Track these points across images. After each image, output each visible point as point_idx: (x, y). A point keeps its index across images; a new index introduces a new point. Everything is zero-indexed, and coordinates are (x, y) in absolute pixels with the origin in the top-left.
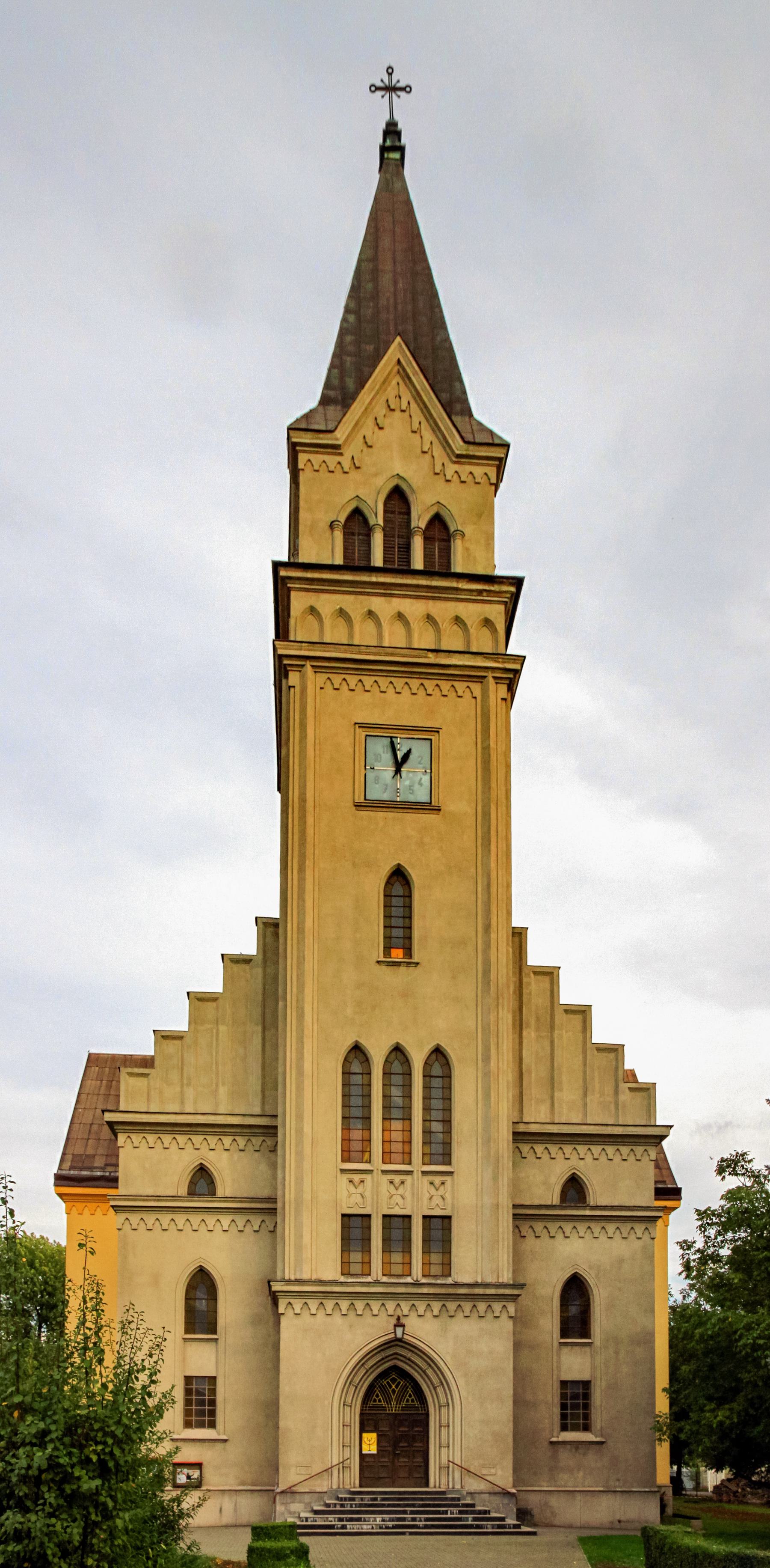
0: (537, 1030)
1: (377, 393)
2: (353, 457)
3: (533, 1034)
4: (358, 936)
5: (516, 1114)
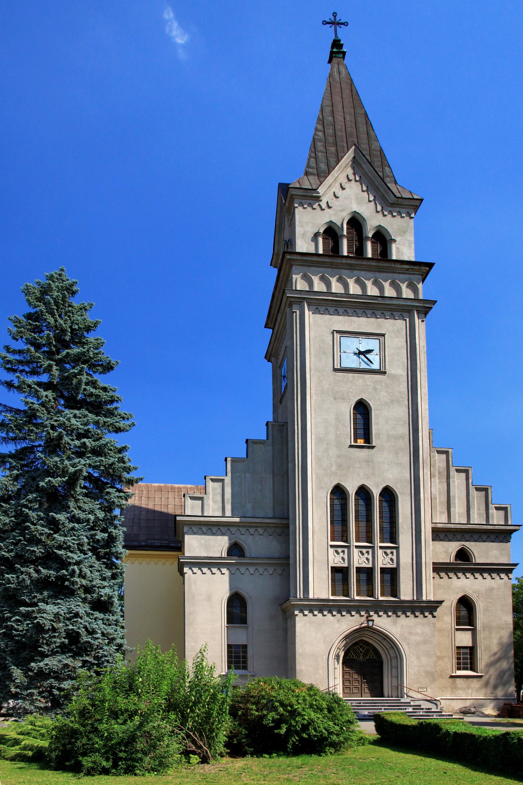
2: (327, 202)
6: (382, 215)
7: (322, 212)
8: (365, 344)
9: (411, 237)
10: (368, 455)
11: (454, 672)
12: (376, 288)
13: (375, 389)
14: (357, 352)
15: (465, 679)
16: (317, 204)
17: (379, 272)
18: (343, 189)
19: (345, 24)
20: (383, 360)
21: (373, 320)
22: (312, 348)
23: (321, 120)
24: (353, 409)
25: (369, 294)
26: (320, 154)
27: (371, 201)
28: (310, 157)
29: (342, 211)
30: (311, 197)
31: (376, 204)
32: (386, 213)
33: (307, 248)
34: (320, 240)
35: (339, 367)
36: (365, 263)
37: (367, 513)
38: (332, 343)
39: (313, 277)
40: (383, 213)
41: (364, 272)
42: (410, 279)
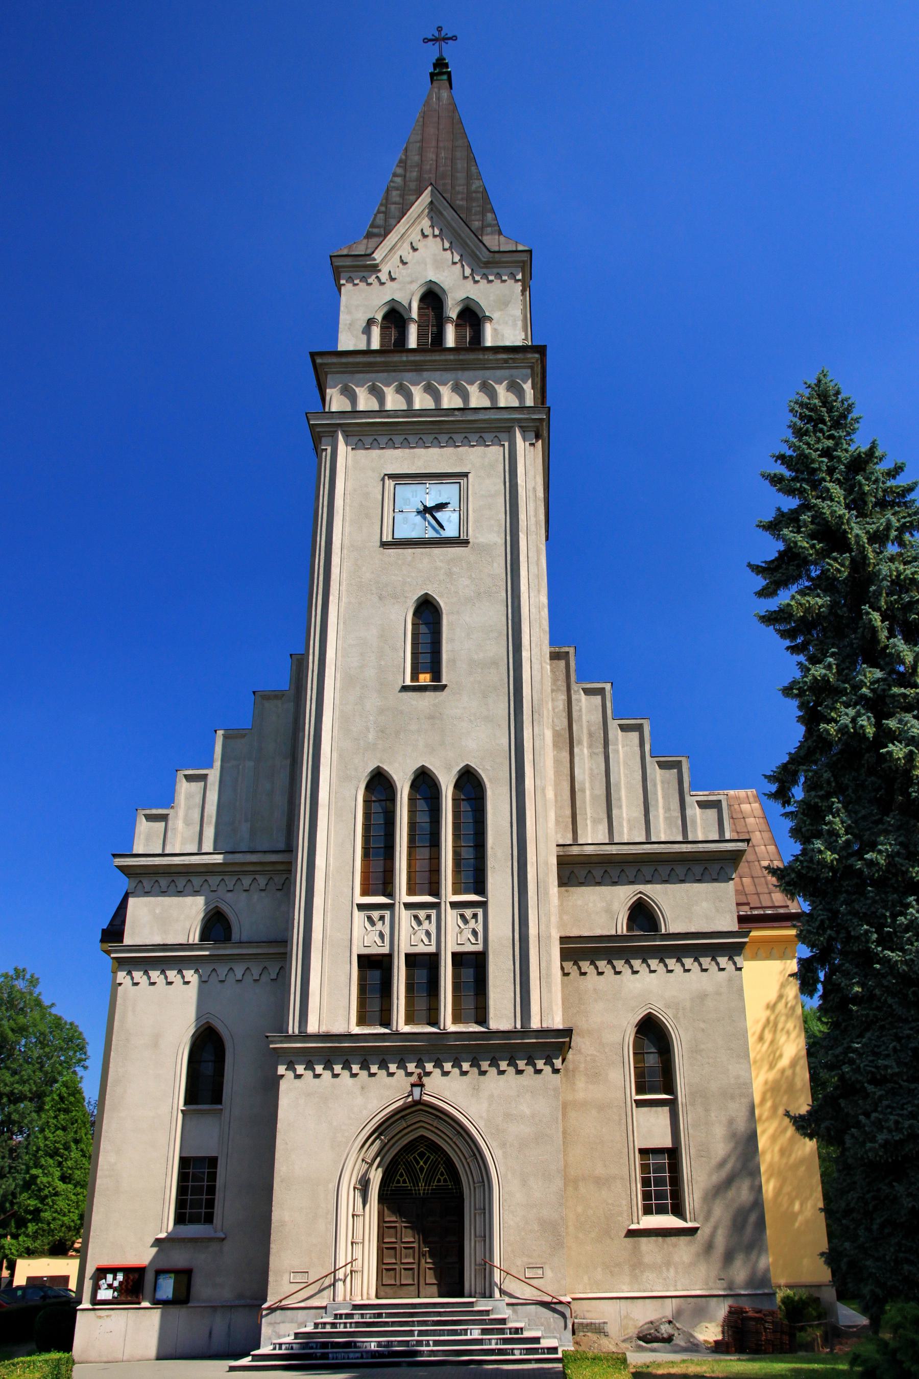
0: (590, 746)
1: (413, 224)
3: (586, 751)
7: (381, 287)
8: (432, 495)
9: (516, 310)
11: (635, 1220)
12: (457, 397)
13: (450, 574)
14: (421, 508)
15: (660, 1239)
16: (374, 276)
17: (464, 369)
18: (415, 250)
19: (454, 38)
20: (463, 522)
21: (450, 450)
22: (347, 508)
23: (403, 163)
25: (445, 407)
26: (393, 207)
28: (379, 212)
29: (411, 282)
30: (364, 268)
31: (463, 266)
32: (477, 278)
33: (355, 345)
34: (376, 331)
35: (390, 539)
36: (437, 358)
37: (432, 828)
38: (380, 497)
39: (357, 390)
41: (439, 373)
42: (512, 376)
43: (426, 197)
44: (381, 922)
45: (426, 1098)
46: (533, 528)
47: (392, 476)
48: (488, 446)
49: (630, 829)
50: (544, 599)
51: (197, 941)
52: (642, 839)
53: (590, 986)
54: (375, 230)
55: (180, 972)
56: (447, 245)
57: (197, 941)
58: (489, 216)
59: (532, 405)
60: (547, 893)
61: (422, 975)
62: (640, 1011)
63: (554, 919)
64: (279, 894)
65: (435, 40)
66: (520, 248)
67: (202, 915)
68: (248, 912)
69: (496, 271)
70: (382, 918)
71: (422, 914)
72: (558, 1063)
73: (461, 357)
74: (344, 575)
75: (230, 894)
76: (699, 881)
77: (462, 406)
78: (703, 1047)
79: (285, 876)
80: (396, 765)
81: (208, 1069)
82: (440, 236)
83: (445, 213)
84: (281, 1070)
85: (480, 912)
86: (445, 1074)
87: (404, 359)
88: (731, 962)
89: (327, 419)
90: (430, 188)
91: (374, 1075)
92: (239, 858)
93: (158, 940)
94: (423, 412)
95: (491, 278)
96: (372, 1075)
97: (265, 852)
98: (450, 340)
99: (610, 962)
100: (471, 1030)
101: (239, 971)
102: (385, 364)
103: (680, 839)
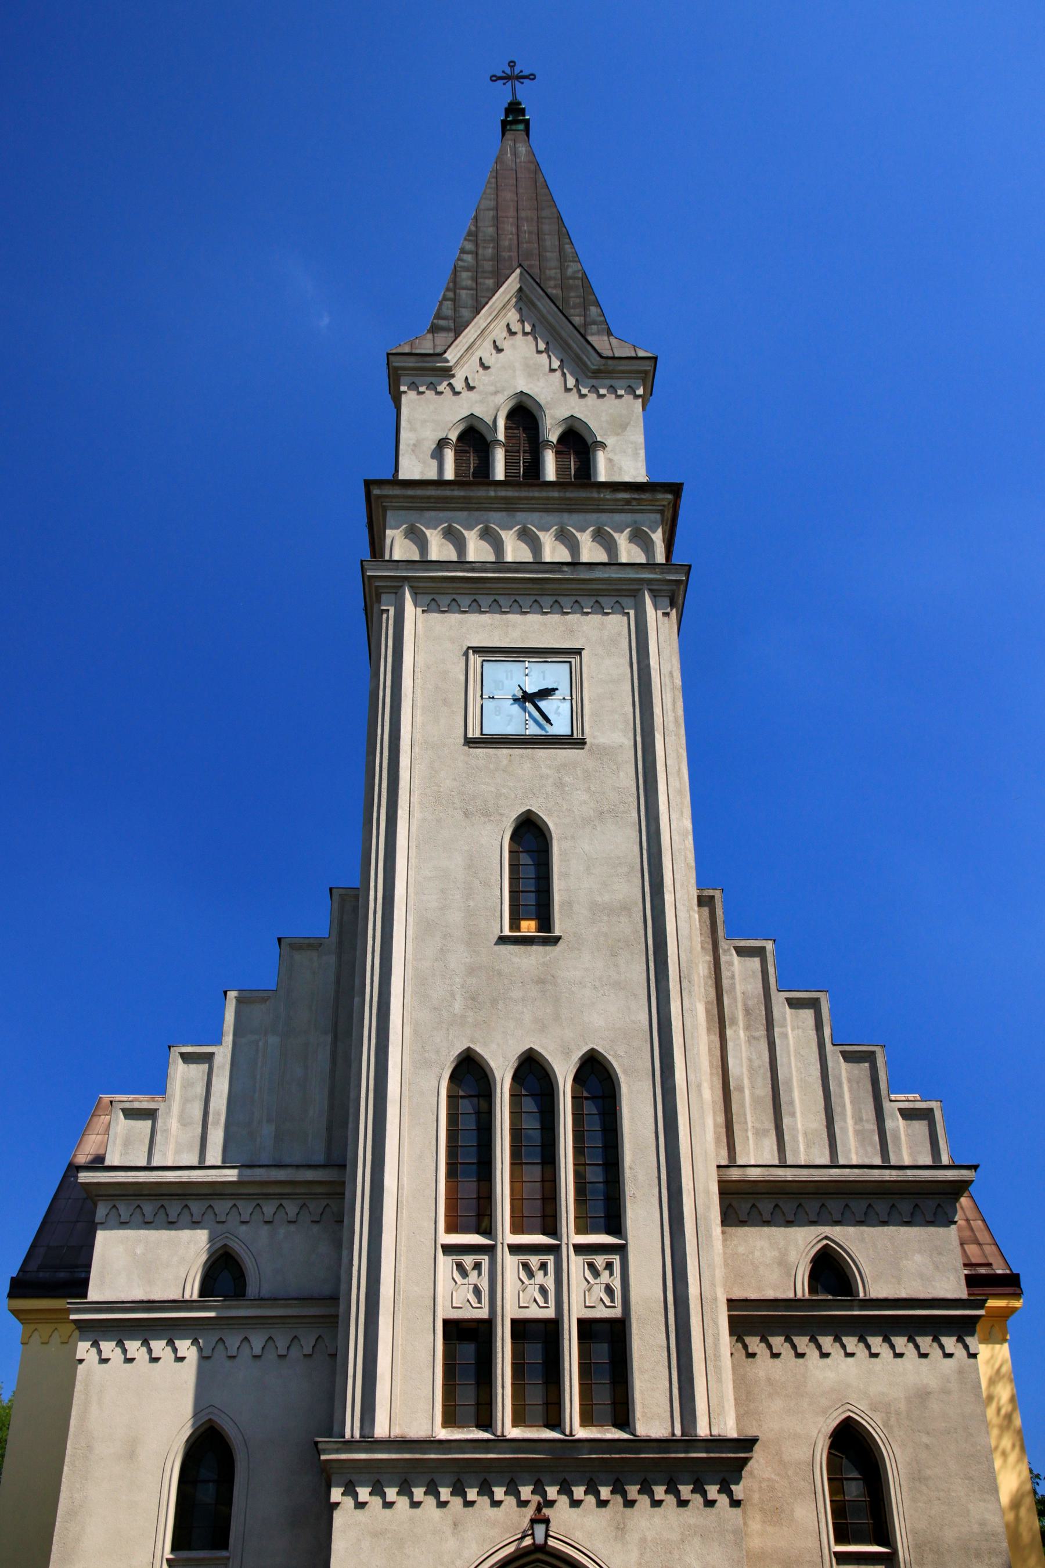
1: (496, 316)
2: (467, 378)
3: (742, 1033)
4: (472, 904)
5: (724, 1152)
6: (577, 396)
7: (454, 398)
9: (637, 436)
10: (544, 964)
12: (563, 547)
13: (560, 785)
14: (520, 694)
16: (445, 383)
17: (570, 511)
18: (499, 350)
19: (532, 77)
20: (577, 714)
21: (555, 618)
22: (418, 691)
23: (473, 236)
24: (512, 838)
25: (548, 560)
26: (463, 293)
27: (554, 370)
28: (445, 299)
29: (496, 393)
30: (433, 371)
31: (564, 375)
32: (584, 391)
33: (422, 473)
34: (449, 455)
35: (478, 735)
36: (537, 494)
37: (544, 1140)
38: (463, 678)
39: (428, 532)
40: (579, 391)
41: (537, 514)
42: (635, 522)
43: (512, 283)
44: (476, 1272)
45: (551, 1542)
46: (671, 726)
47: (478, 650)
48: (608, 614)
49: (808, 1146)
50: (688, 824)
51: (195, 1297)
52: (825, 1160)
53: (762, 1374)
54: (442, 323)
55: (171, 1343)
56: (542, 346)
57: (195, 1297)
58: (593, 310)
59: (664, 562)
60: (709, 1236)
61: (535, 1353)
62: (835, 1414)
63: (719, 1273)
64: (316, 1228)
65: (507, 78)
66: (641, 354)
67: (204, 1257)
68: (274, 1256)
69: (608, 382)
70: (477, 1266)
71: (534, 1261)
72: (738, 1490)
73: (568, 495)
74: (416, 783)
75: (244, 1228)
76: (908, 1223)
77: (570, 560)
78: (929, 1472)
79: (324, 1203)
80: (494, 1046)
81: (207, 1494)
82: (533, 333)
83: (539, 304)
84: (336, 1494)
85: (616, 1260)
86: (575, 1504)
87: (492, 494)
88: (960, 1345)
89: (391, 570)
90: (518, 271)
91: (471, 1504)
92: (260, 1174)
93: (138, 1294)
94: (519, 566)
95: (602, 391)
96: (469, 1504)
97: (298, 1166)
98: (550, 473)
99: (788, 1339)
100: (609, 1436)
101: (257, 1343)
102: (467, 500)
103: (878, 1161)
